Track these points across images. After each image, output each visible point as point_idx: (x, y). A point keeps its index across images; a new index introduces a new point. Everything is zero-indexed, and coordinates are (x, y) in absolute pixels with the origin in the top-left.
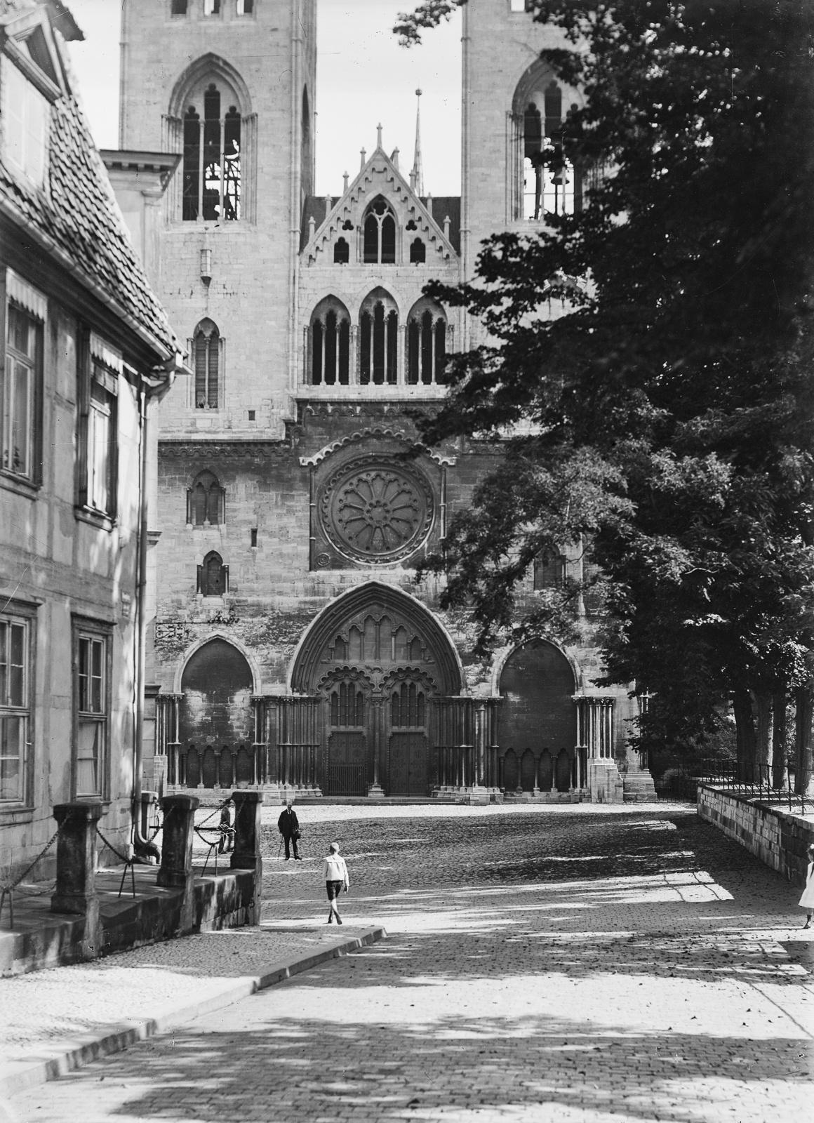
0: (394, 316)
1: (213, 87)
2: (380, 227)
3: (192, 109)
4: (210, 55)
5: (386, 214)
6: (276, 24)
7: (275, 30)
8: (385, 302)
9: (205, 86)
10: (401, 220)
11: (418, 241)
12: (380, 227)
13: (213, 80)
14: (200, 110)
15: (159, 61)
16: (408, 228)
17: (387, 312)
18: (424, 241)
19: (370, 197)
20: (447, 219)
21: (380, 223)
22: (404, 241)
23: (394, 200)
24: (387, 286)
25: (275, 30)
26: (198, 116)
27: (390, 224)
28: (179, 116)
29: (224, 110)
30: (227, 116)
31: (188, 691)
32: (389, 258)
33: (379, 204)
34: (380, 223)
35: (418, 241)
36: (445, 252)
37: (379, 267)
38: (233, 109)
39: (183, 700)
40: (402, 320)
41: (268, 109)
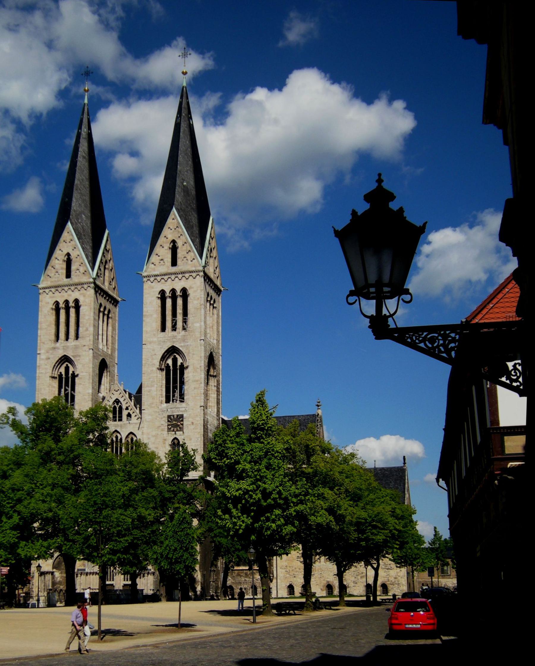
0: (121, 439)
1: (67, 365)
2: (118, 409)
3: (61, 373)
4: (65, 355)
5: (120, 404)
6: (84, 344)
7: (85, 346)
8: (118, 435)
9: (65, 365)
10: (124, 407)
11: (129, 413)
12: (118, 409)
13: (67, 363)
14: (63, 373)
15: (49, 359)
16: (126, 409)
17: (119, 438)
18: (131, 413)
19: (114, 399)
20: (138, 406)
21: (117, 408)
22: (125, 413)
23: (121, 400)
24: (118, 430)
25: (85, 346)
26: (62, 375)
27: (121, 408)
28: (56, 376)
29: (71, 372)
30: (72, 374)
31: (54, 570)
32: (120, 420)
33: (117, 401)
34: (117, 408)
35: (129, 413)
36: (137, 417)
37: (117, 423)
38: (73, 372)
39: (52, 573)
40: (123, 441)
41: (82, 372)
